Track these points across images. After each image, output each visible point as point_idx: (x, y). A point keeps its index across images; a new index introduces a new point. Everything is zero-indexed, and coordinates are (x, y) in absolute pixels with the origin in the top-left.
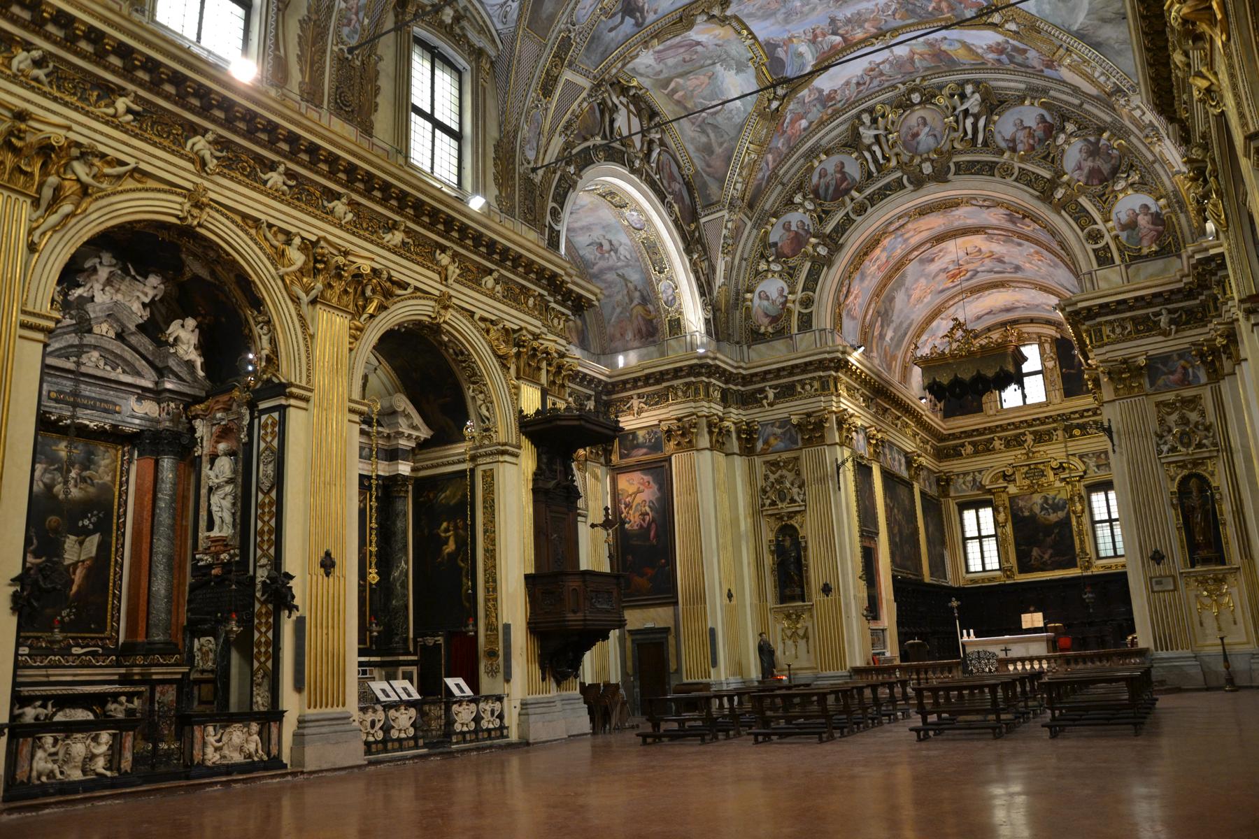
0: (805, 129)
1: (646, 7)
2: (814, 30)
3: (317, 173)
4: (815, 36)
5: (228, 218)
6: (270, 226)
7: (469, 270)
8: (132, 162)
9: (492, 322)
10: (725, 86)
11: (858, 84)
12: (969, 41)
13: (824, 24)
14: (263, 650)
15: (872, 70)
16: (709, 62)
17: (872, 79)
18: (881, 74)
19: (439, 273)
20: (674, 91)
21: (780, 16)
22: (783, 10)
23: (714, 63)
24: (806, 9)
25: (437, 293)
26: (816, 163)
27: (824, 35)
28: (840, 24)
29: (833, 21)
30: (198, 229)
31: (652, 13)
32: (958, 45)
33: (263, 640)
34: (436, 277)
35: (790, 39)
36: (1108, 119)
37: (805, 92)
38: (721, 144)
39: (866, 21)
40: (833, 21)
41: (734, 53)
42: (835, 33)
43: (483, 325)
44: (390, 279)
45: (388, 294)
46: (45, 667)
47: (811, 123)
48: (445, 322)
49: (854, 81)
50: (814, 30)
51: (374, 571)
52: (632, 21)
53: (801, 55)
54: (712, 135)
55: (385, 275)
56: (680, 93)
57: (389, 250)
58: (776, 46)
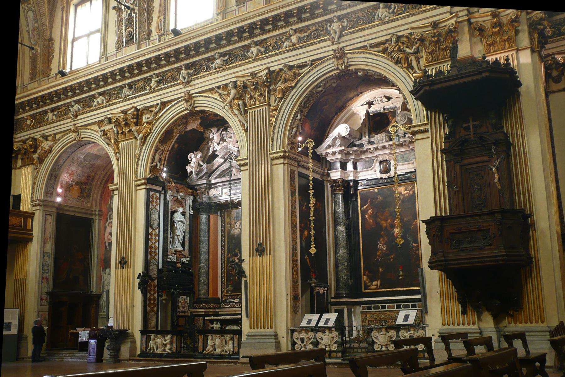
3: (235, 43)
5: (202, 96)
6: (219, 87)
7: (360, 18)
8: (159, 102)
9: (387, 41)
14: (152, 302)
19: (329, 39)
25: (332, 52)
30: (196, 109)
33: (152, 297)
34: (329, 43)
43: (381, 49)
44: (291, 68)
45: (296, 75)
46: (229, 308)
48: (347, 67)
51: (313, 246)
55: (285, 69)
57: (288, 51)
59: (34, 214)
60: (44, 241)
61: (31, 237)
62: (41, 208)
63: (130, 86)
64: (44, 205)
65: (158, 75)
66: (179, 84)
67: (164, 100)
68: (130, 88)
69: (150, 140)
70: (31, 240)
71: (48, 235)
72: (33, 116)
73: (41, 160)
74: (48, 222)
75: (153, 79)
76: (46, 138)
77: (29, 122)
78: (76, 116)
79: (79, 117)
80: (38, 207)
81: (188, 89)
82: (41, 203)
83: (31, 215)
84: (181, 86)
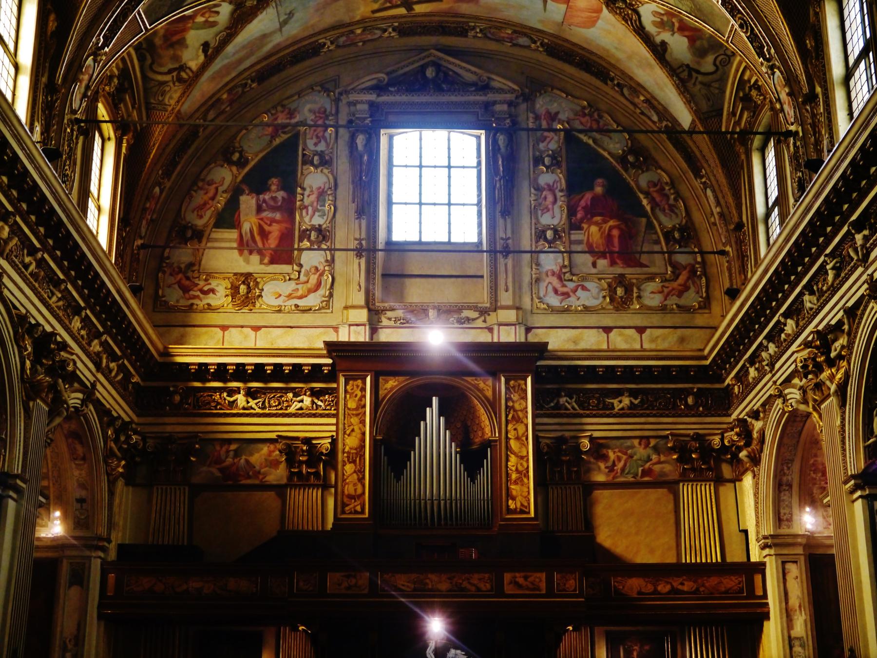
59: (763, 564)
60: (788, 615)
61: (766, 610)
62: (772, 552)
63: (809, 288)
64: (776, 545)
65: (832, 255)
66: (855, 268)
67: (850, 304)
68: (812, 293)
69: (851, 391)
70: (767, 616)
71: (794, 601)
72: (737, 377)
73: (755, 460)
74: (790, 578)
75: (828, 267)
76: (755, 415)
77: (736, 388)
78: (772, 365)
79: (777, 366)
80: (767, 551)
81: (870, 271)
82: (769, 541)
83: (760, 568)
84: (860, 270)
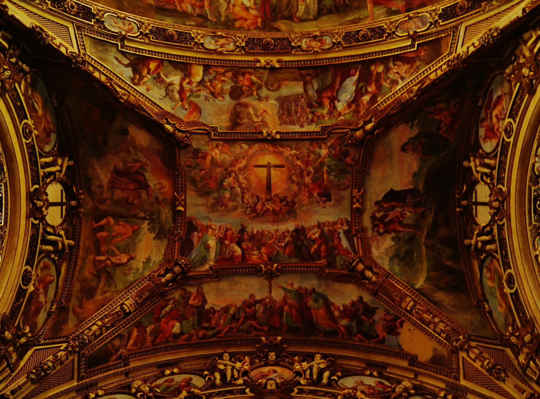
0: (176, 336)
1: (145, 79)
2: (227, 229)
4: (225, 237)
10: (140, 245)
11: (234, 318)
12: (332, 299)
13: (236, 229)
15: (249, 306)
16: (142, 215)
17: (246, 318)
18: (253, 316)
20: (101, 229)
21: (211, 201)
22: (215, 195)
23: (144, 219)
24: (231, 204)
26: (168, 372)
27: (231, 242)
28: (246, 237)
29: (243, 230)
31: (145, 88)
32: (321, 302)
35: (208, 227)
36: (442, 385)
37: (193, 290)
38: (104, 292)
39: (264, 244)
40: (243, 230)
41: (164, 215)
42: (239, 244)
47: (182, 333)
49: (232, 311)
50: (227, 229)
52: (132, 75)
53: (207, 248)
54: (101, 285)
56: (104, 234)
58: (195, 229)
